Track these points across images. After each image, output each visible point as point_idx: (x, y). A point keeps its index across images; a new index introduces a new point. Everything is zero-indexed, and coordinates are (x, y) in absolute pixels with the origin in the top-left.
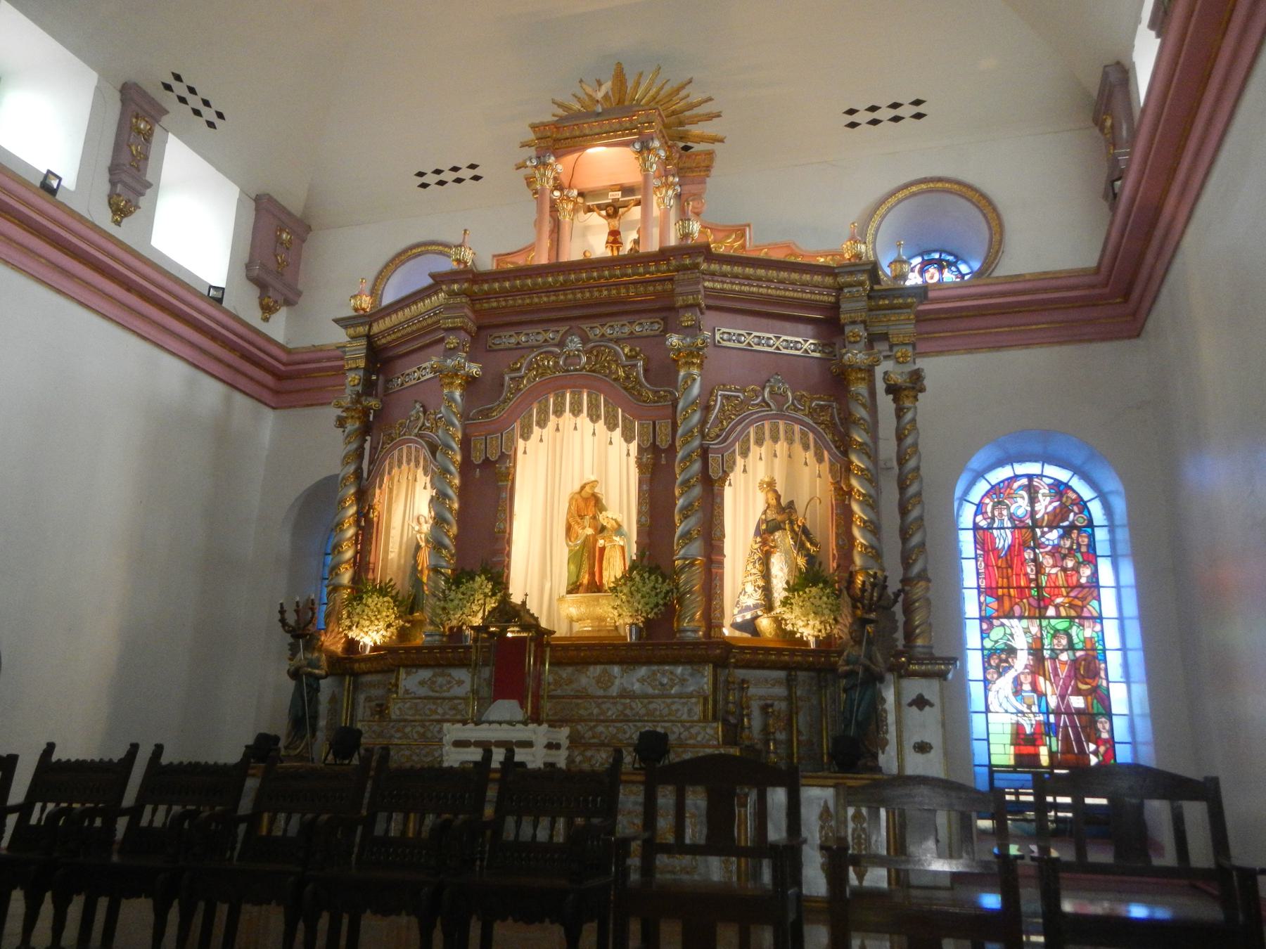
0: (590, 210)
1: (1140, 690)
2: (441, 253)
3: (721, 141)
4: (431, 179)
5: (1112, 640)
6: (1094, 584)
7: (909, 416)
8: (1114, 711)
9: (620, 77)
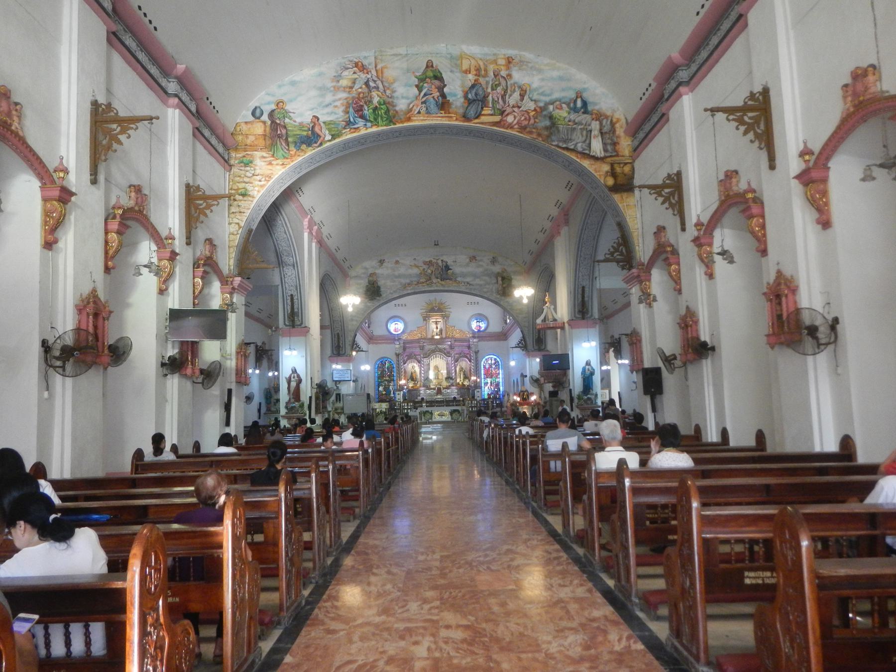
5: (501, 381)
9: (435, 299)
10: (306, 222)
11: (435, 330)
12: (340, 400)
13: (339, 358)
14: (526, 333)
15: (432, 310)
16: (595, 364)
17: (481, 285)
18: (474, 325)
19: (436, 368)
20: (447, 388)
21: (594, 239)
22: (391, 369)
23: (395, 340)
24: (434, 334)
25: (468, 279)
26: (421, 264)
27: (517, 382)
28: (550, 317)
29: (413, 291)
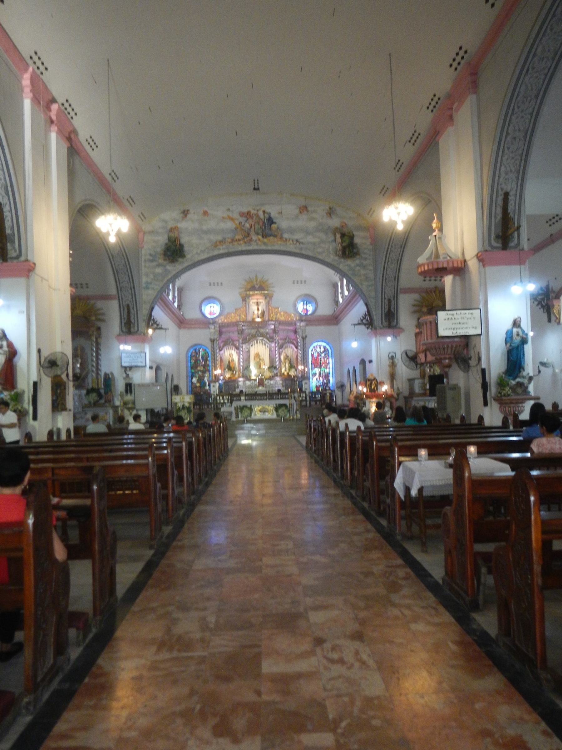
1: (334, 379)
6: (329, 363)
9: (256, 276)
10: (26, 81)
11: (256, 312)
12: (131, 392)
13: (129, 337)
14: (372, 305)
15: (253, 288)
16: (526, 325)
17: (314, 244)
18: (300, 307)
19: (257, 356)
20: (271, 378)
21: (537, 97)
23: (210, 323)
24: (255, 316)
25: (298, 236)
26: (236, 216)
27: (354, 368)
28: (441, 252)
29: (226, 251)
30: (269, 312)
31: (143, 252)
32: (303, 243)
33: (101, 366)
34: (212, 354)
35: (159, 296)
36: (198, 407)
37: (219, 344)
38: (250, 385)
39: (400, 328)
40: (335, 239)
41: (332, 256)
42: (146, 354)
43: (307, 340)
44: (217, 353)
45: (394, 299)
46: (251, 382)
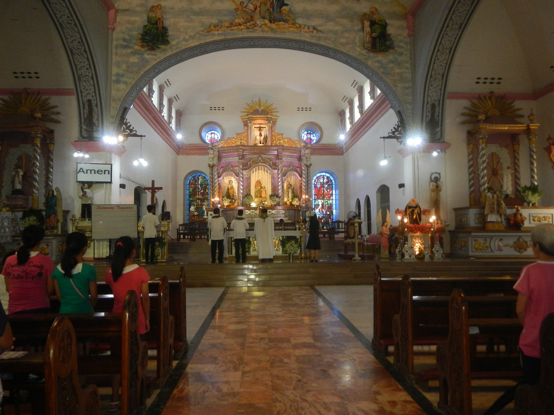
0: (255, 127)
2: (214, 124)
3: (279, 117)
4: (213, 109)
5: (334, 203)
6: (332, 195)
7: (309, 171)
8: (334, 214)
9: (259, 100)
11: (258, 138)
12: (90, 217)
15: (256, 112)
18: (304, 136)
19: (259, 183)
20: (272, 207)
22: (205, 186)
23: (209, 149)
25: (315, 22)
29: (222, 37)
30: (272, 138)
31: (115, 35)
32: (321, 31)
33: (52, 182)
34: (210, 180)
35: (134, 94)
36: (189, 237)
37: (217, 169)
38: (250, 214)
39: (444, 142)
40: (363, 27)
41: (358, 49)
42: (111, 165)
43: (312, 169)
44: (215, 179)
45: (439, 104)
46: (251, 211)
